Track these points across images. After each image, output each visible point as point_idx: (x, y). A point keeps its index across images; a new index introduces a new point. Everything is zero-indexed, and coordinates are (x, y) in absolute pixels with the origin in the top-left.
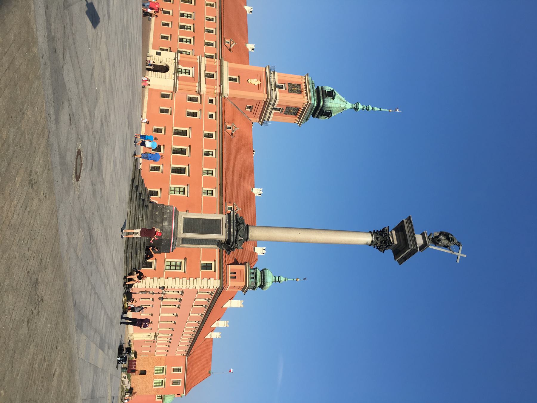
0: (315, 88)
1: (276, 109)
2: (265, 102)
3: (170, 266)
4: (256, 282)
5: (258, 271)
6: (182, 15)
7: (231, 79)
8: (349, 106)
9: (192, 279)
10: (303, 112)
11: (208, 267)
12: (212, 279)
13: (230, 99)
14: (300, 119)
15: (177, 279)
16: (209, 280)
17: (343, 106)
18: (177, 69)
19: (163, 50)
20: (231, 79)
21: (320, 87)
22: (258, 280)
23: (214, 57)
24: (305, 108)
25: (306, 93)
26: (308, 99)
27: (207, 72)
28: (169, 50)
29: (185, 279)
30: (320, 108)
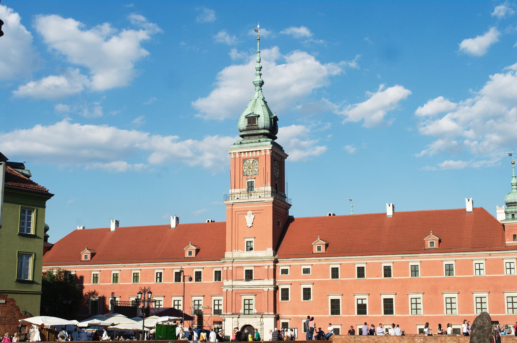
13: (276, 248)
21: (242, 133)
26: (265, 151)
27: (244, 279)
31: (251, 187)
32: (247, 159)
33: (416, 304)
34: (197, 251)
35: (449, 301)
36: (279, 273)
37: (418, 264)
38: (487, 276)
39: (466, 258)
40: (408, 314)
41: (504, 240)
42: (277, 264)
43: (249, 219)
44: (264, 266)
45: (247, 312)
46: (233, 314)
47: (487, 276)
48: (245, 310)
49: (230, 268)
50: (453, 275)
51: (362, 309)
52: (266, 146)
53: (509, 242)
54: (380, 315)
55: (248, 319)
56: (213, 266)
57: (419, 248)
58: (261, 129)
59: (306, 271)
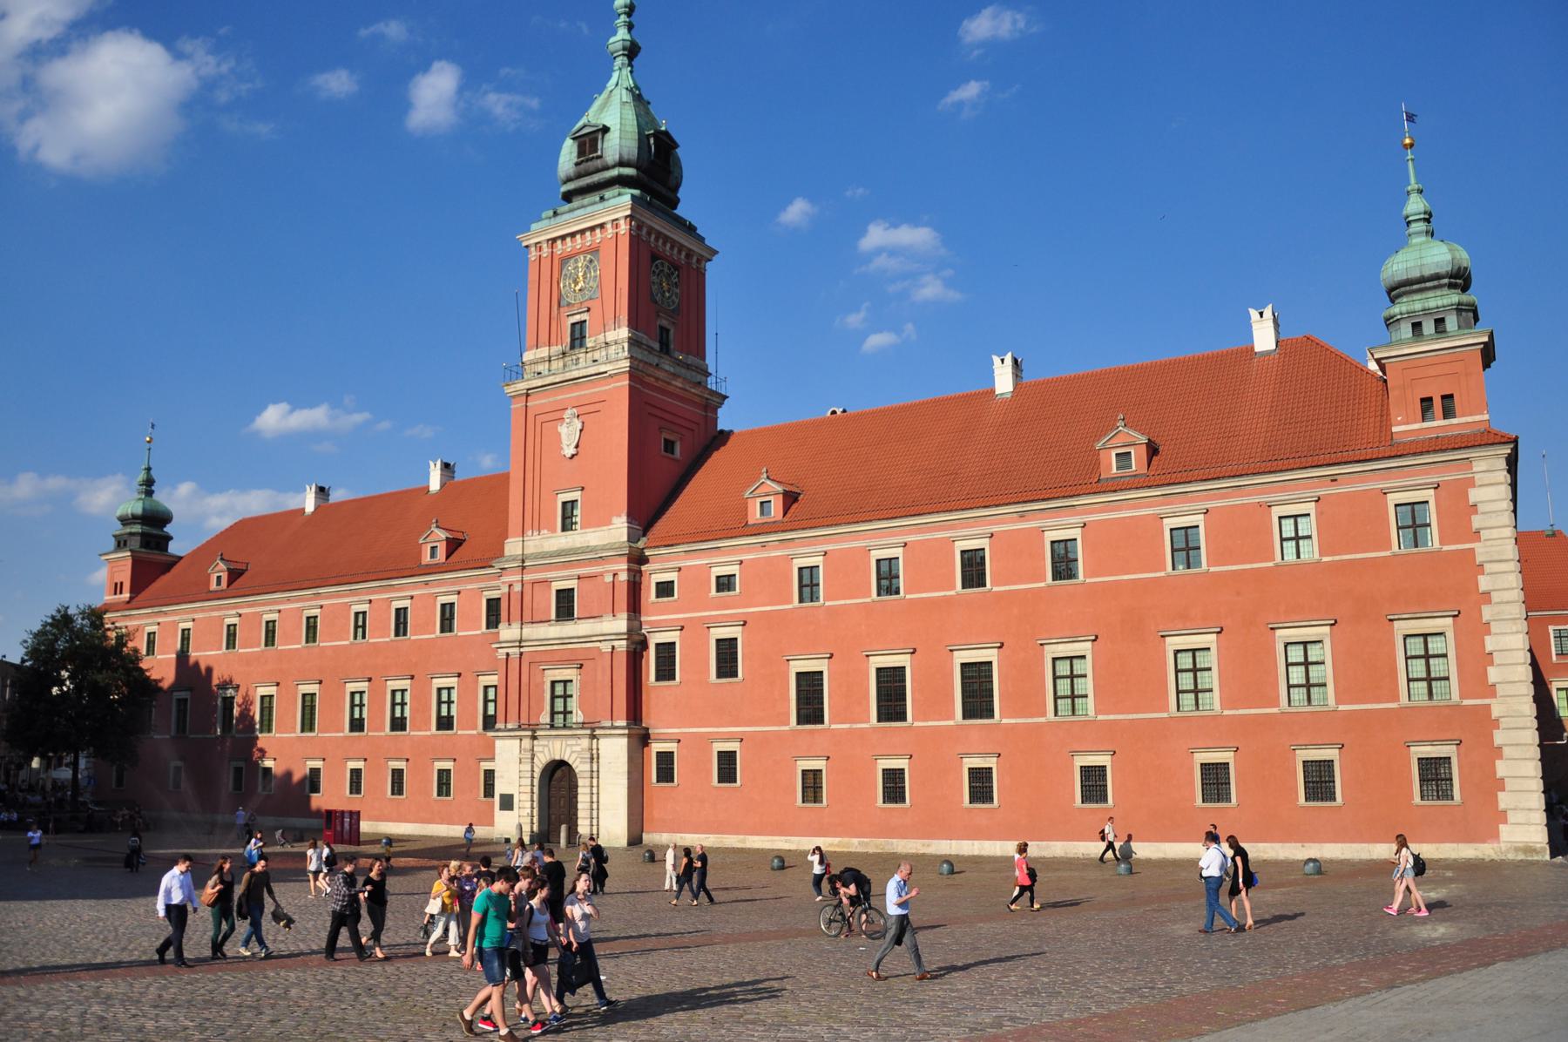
0: (567, 207)
1: (665, 348)
2: (642, 383)
3: (1429, 680)
4: (1459, 309)
5: (1404, 309)
6: (357, 725)
7: (567, 525)
8: (620, 78)
9: (1484, 583)
10: (666, 239)
11: (1414, 524)
12: (1474, 495)
14: (689, 254)
15: (1490, 644)
16: (1481, 508)
17: (626, 97)
18: (552, 727)
19: (489, 790)
20: (567, 525)
21: (564, 189)
22: (1446, 301)
23: (494, 594)
24: (650, 231)
25: (592, 229)
27: (553, 616)
28: (486, 765)
29: (1487, 613)
30: (645, 178)
31: (578, 336)
32: (569, 257)
33: (1072, 677)
34: (453, 545)
35: (1186, 661)
36: (650, 594)
37: (1075, 533)
38: (1325, 559)
39: (1246, 500)
40: (1044, 714)
41: (1385, 420)
42: (643, 568)
43: (568, 433)
44: (601, 574)
45: (559, 719)
46: (520, 728)
47: (1325, 559)
48: (553, 713)
49: (517, 588)
50: (1199, 564)
51: (892, 701)
52: (616, 209)
53: (1406, 427)
54: (951, 723)
55: (558, 743)
56: (482, 585)
57: (1080, 479)
58: (614, 167)
59: (725, 583)
